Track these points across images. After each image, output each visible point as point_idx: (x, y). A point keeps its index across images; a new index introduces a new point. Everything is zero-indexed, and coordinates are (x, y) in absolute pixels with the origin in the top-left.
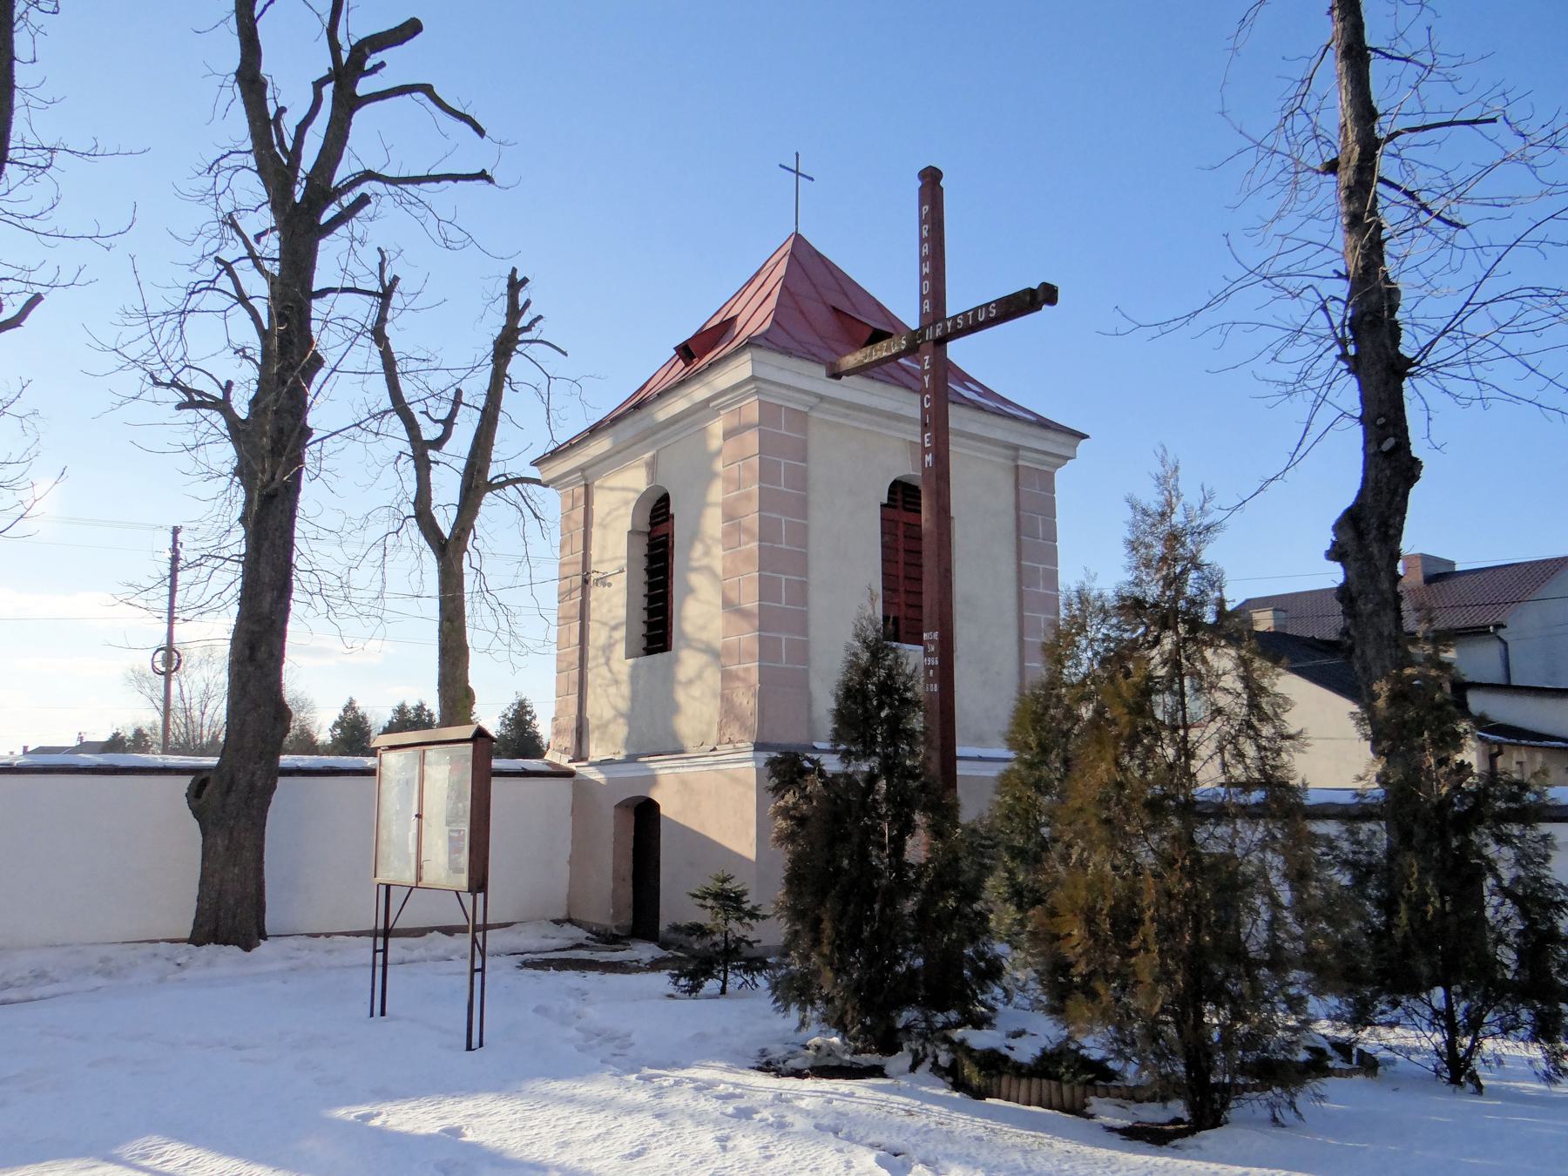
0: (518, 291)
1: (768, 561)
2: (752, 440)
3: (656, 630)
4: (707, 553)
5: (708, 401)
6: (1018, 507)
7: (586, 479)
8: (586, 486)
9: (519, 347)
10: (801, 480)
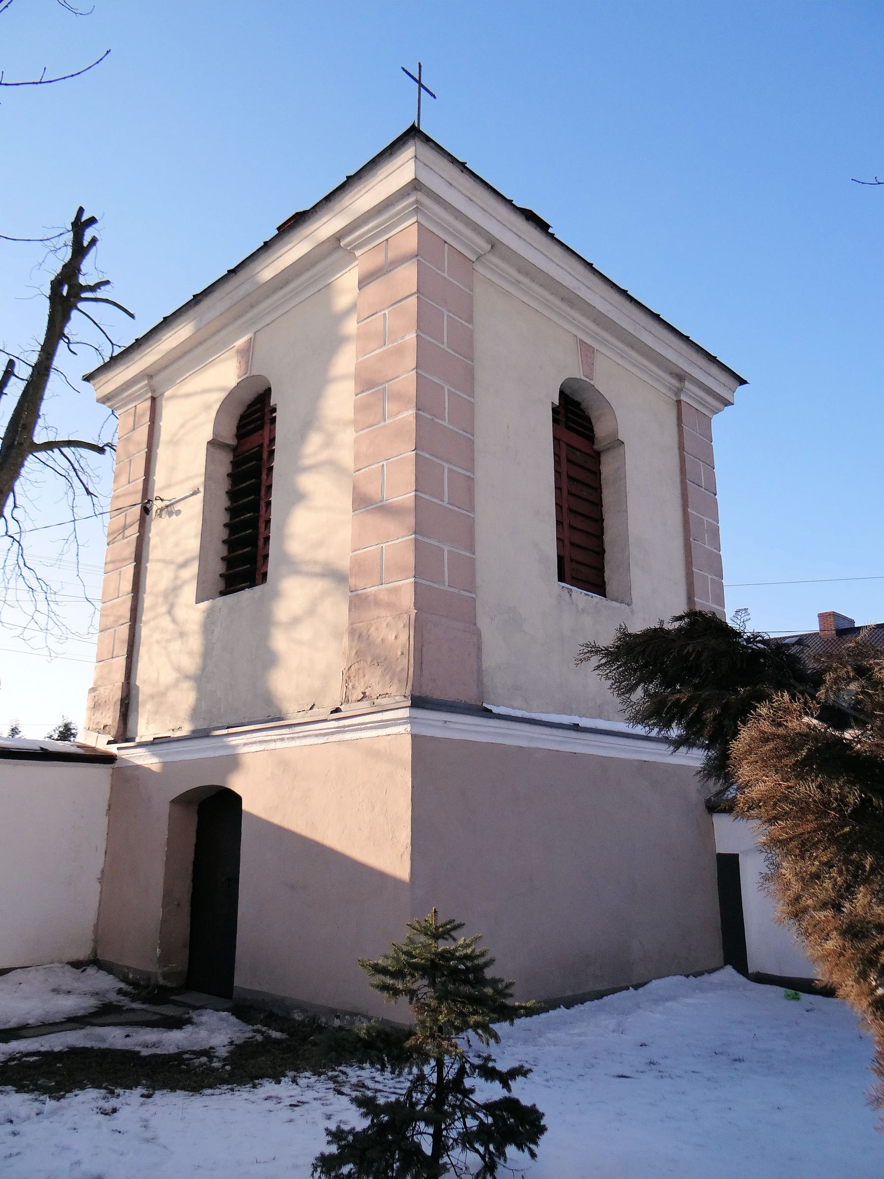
0: (84, 231)
1: (426, 437)
2: (407, 276)
3: (243, 555)
4: (329, 442)
5: (338, 237)
6: (681, 447)
7: (153, 391)
8: (153, 399)
9: (80, 305)
10: (466, 345)
